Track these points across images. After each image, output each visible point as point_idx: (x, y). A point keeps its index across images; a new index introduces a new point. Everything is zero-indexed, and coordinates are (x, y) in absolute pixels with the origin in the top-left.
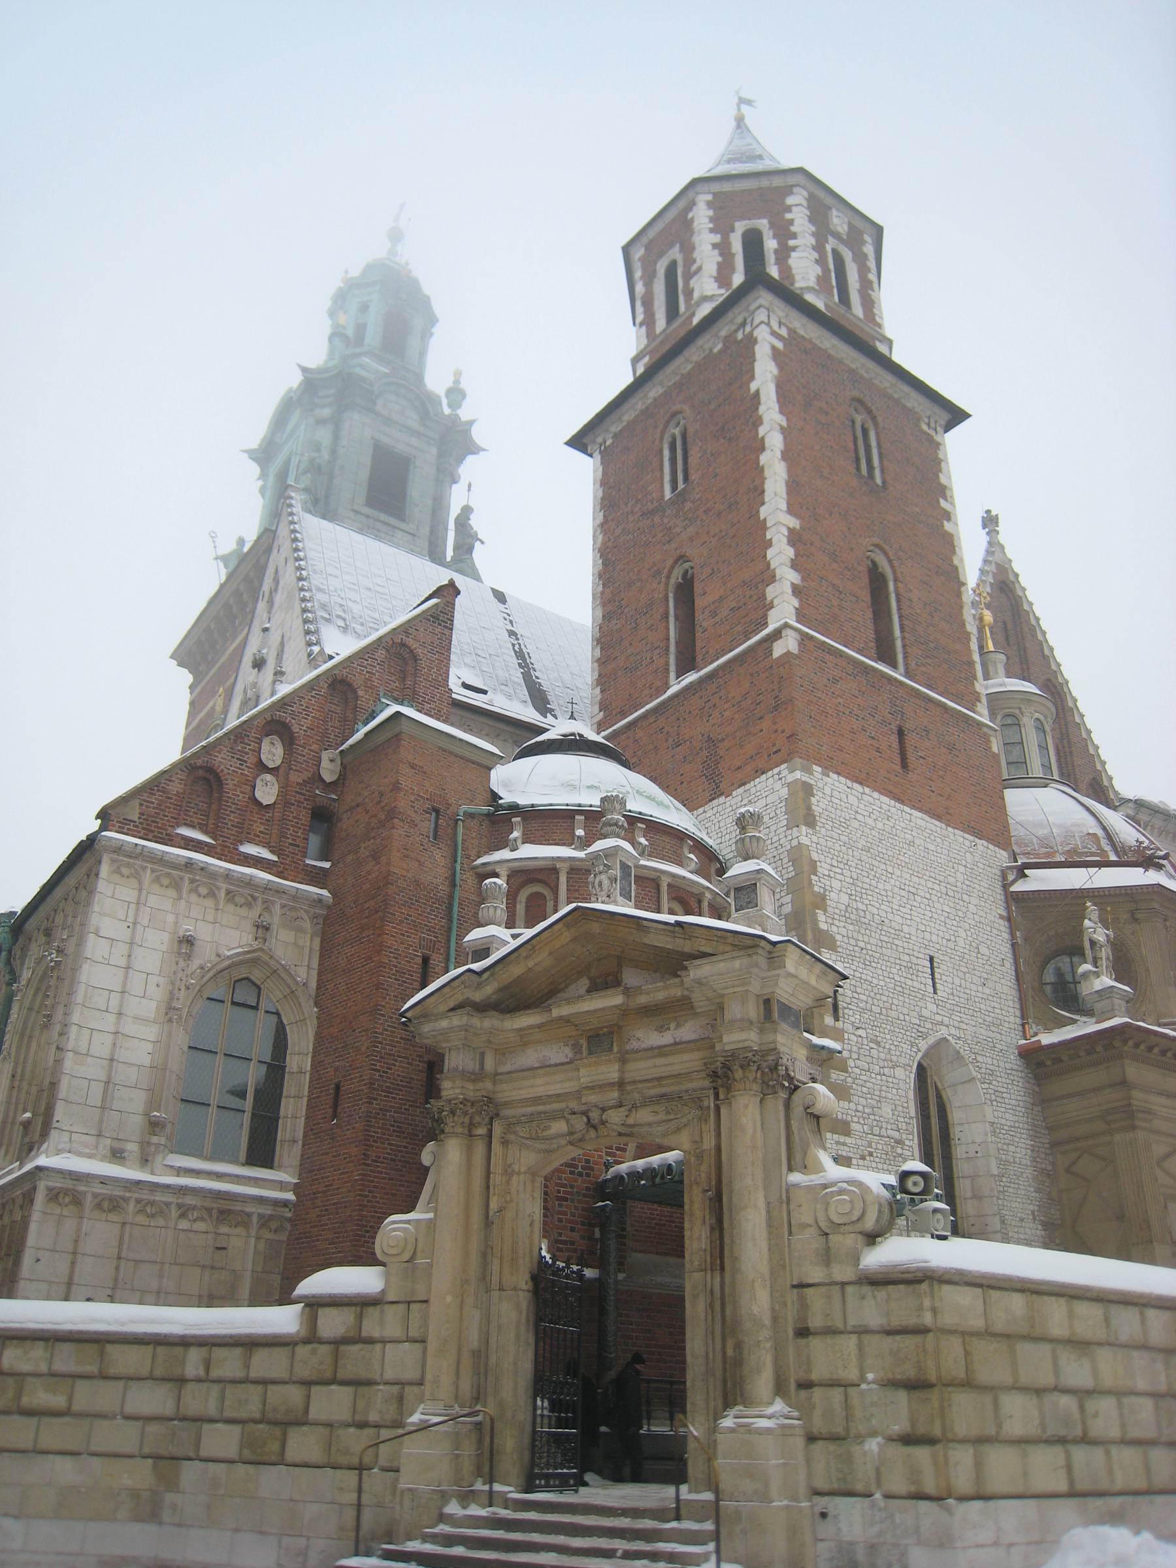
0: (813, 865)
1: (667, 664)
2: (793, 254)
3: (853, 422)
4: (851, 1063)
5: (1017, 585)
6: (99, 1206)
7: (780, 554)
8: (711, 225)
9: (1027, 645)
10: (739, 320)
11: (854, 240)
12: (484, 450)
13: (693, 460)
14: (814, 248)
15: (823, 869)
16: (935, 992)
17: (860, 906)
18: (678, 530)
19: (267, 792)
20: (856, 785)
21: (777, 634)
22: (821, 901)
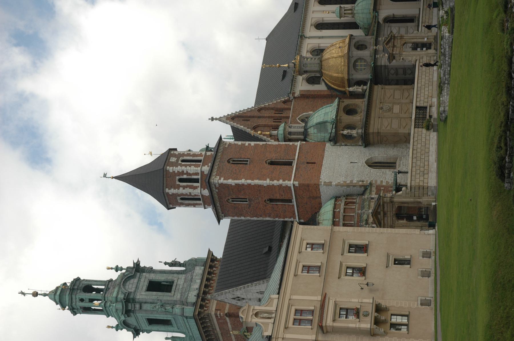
0: (338, 183)
1: (288, 205)
2: (189, 172)
3: (232, 163)
4: (371, 179)
7: (275, 183)
8: (177, 189)
9: (249, 115)
10: (214, 186)
11: (175, 156)
12: (138, 260)
13: (242, 197)
14: (186, 167)
15: (339, 181)
17: (344, 175)
18: (258, 201)
20: (322, 173)
21: (294, 185)
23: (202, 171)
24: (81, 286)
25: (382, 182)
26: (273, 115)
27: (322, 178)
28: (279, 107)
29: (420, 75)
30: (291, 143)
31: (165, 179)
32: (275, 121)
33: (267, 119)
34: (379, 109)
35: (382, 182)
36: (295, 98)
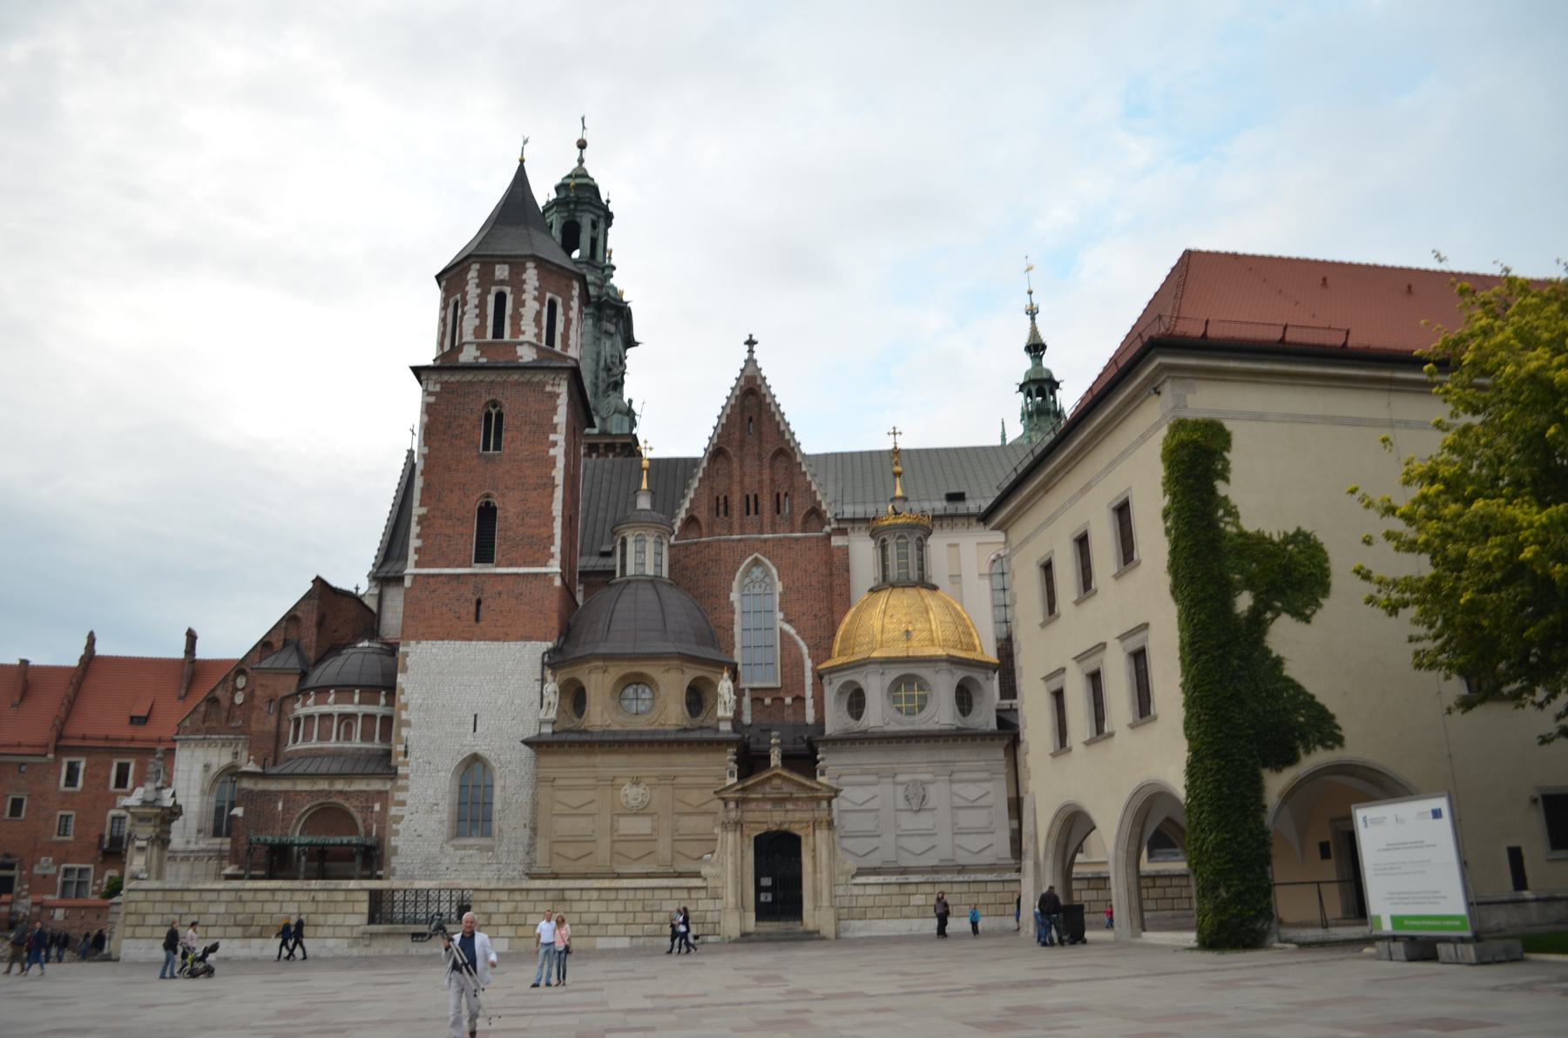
2: (465, 317)
5: (763, 387)
6: (182, 859)
9: (763, 430)
14: (476, 307)
16: (475, 730)
19: (239, 699)
22: (405, 706)
23: (466, 348)
24: (578, 214)
25: (403, 803)
26: (766, 491)
27: (420, 646)
28: (796, 501)
29: (622, 895)
30: (556, 549)
31: (457, 270)
32: (752, 498)
33: (757, 478)
34: (629, 774)
35: (403, 803)
36: (829, 536)
